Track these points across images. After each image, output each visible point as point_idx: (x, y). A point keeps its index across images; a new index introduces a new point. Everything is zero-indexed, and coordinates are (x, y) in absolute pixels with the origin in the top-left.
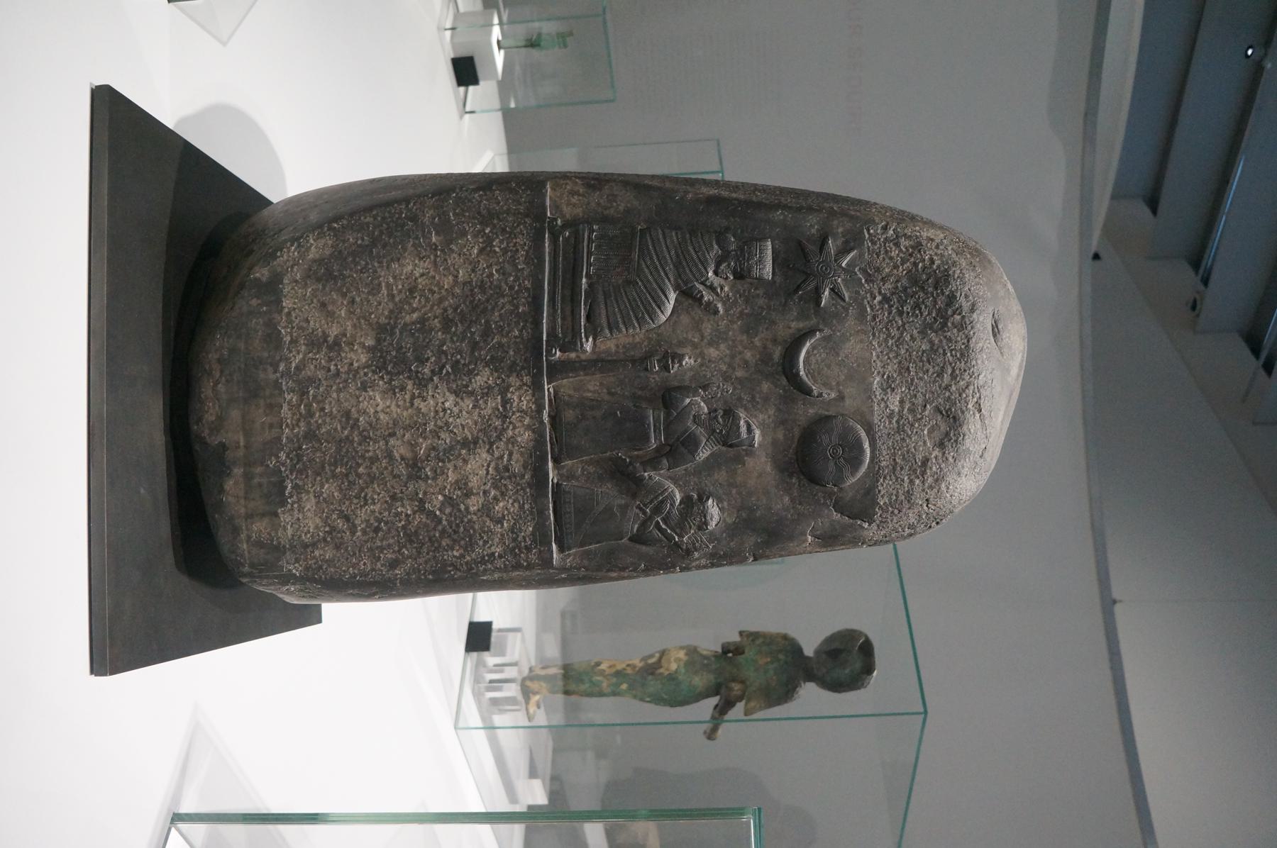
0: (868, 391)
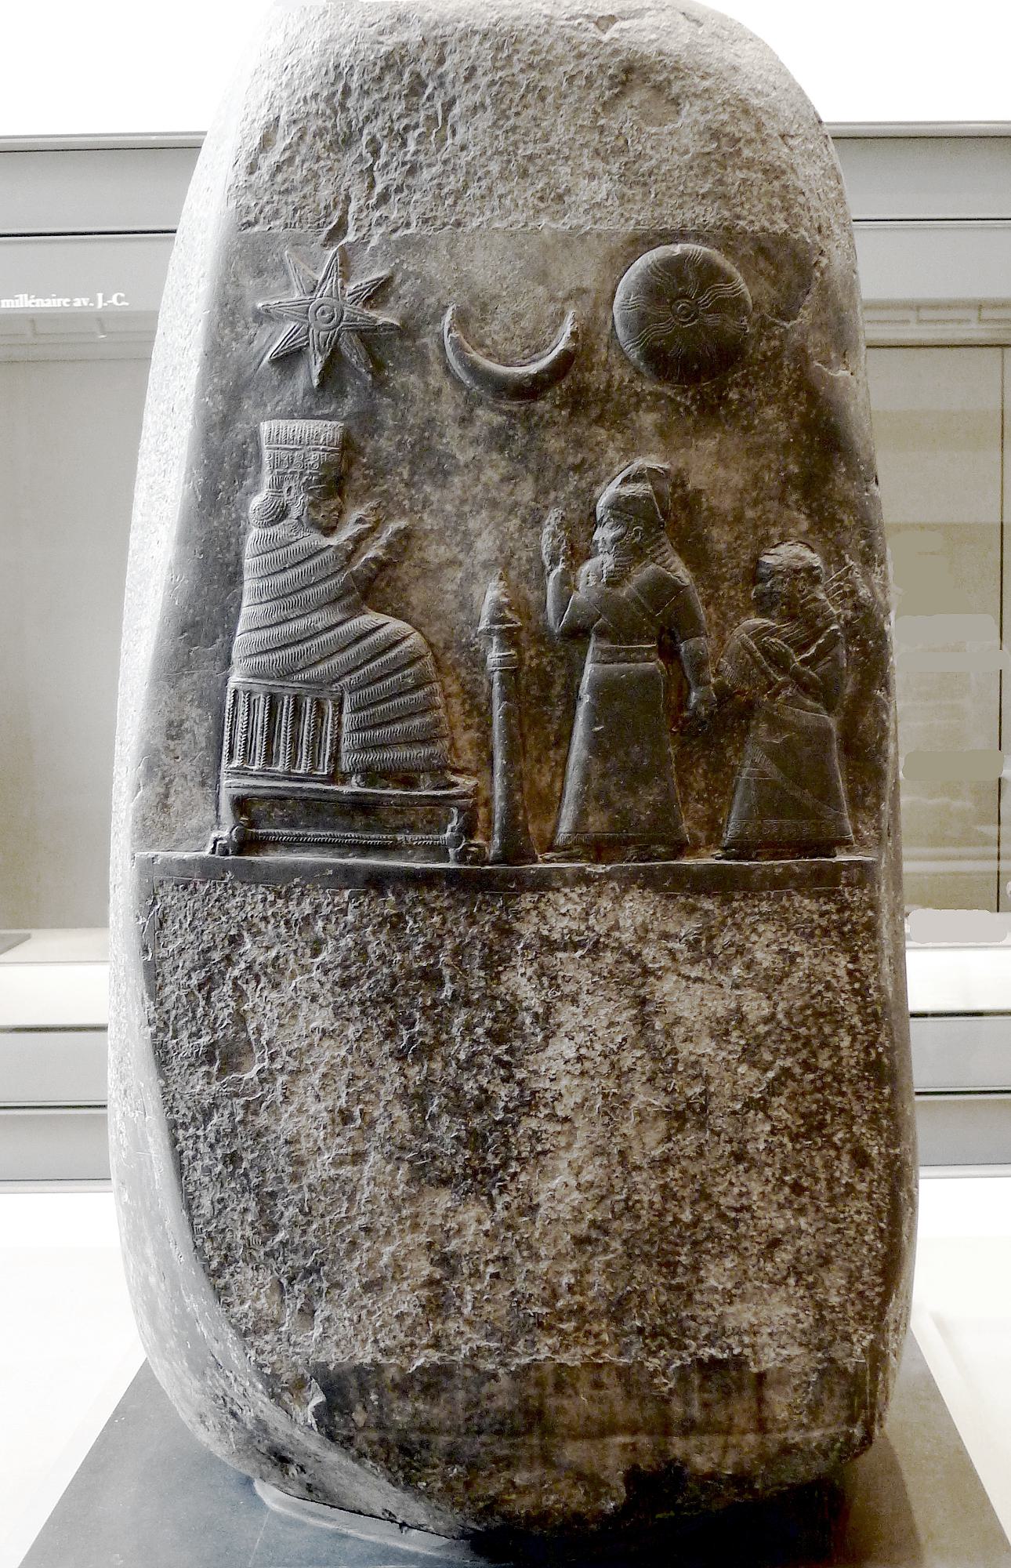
0: (570, 240)
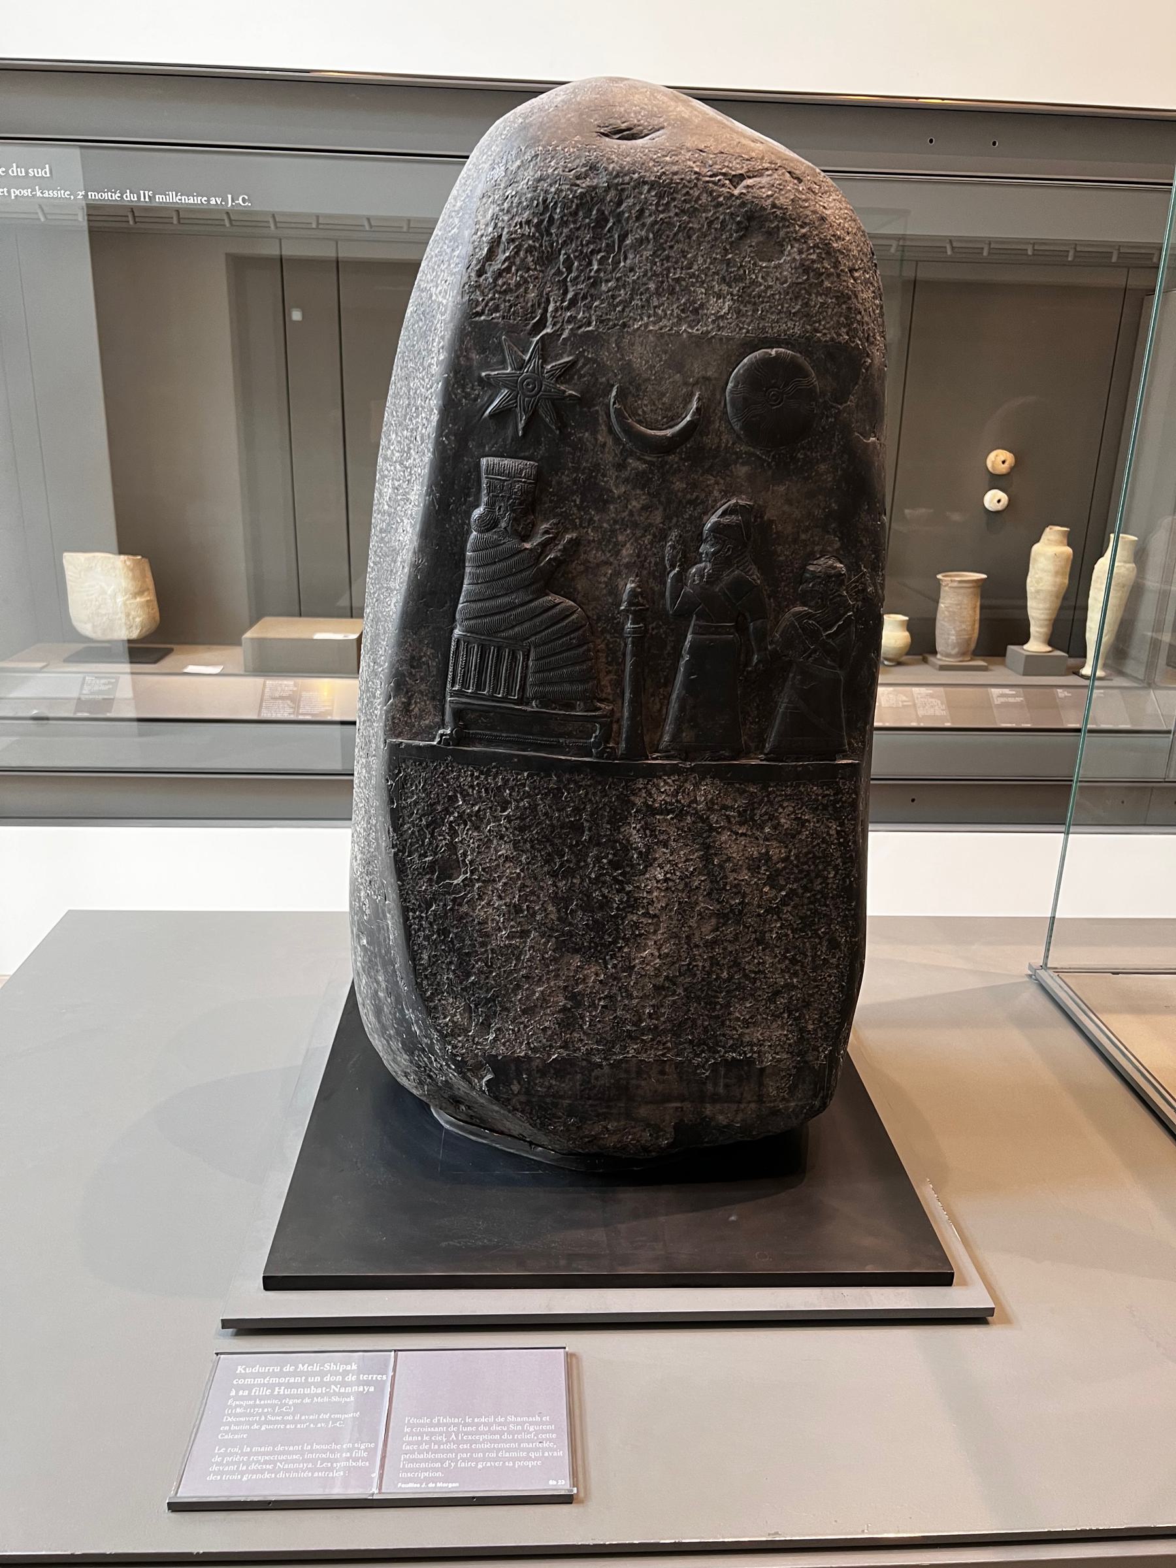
0: (702, 341)
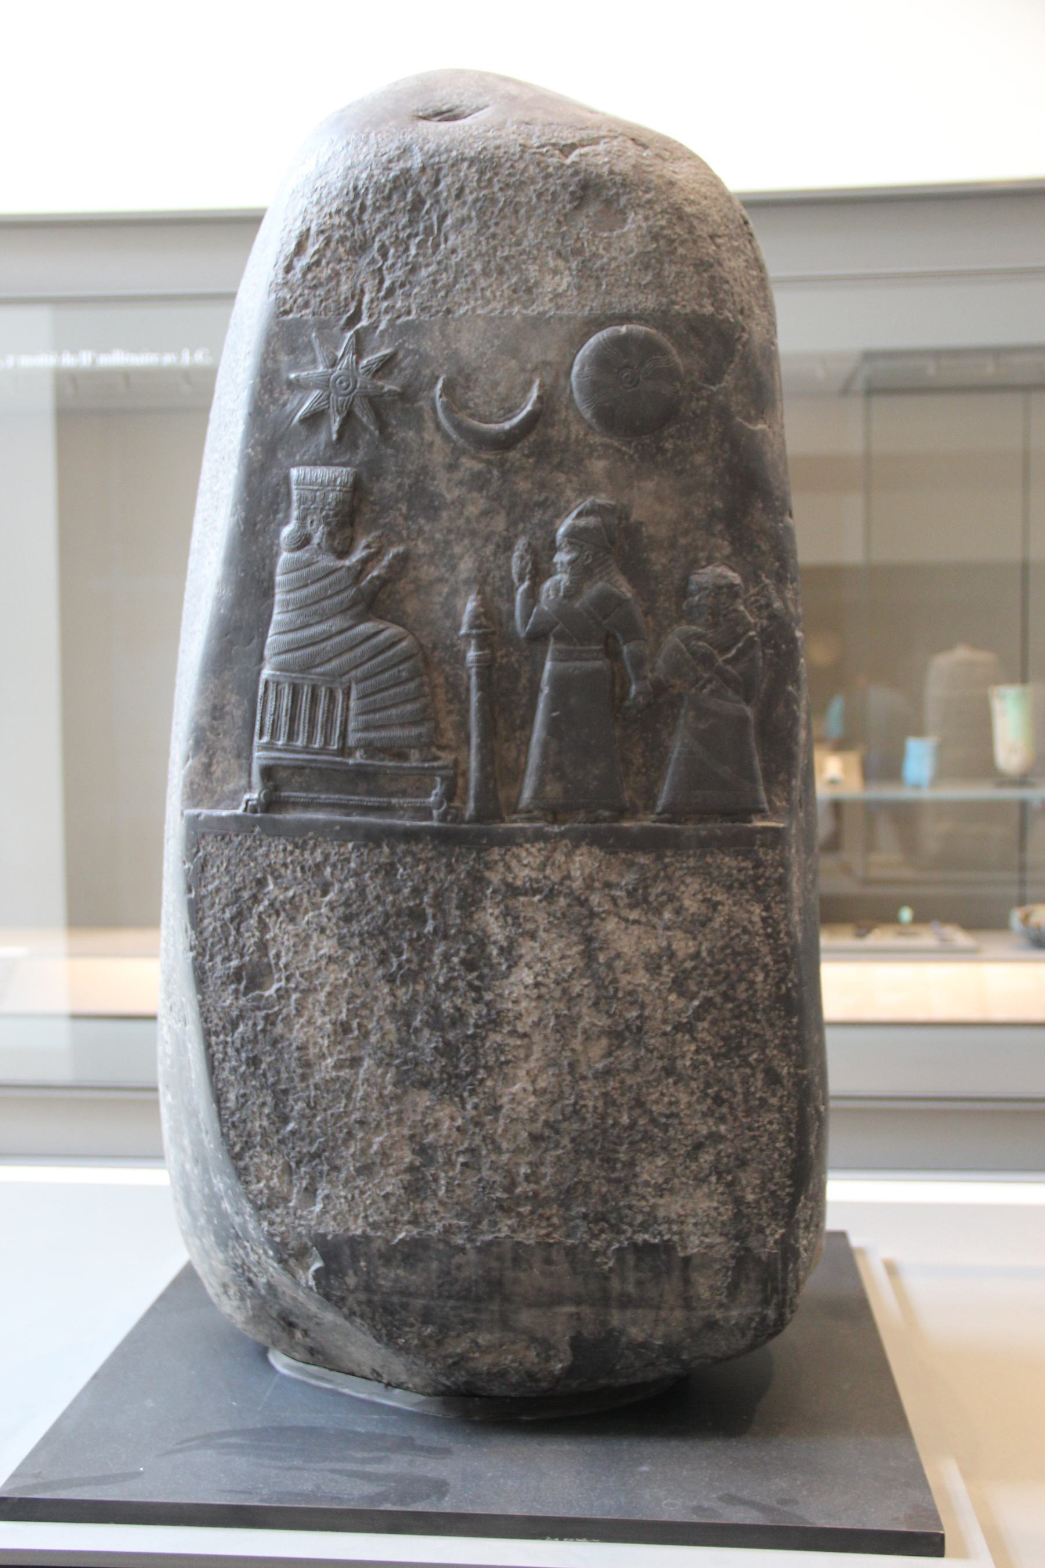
0: (538, 322)
